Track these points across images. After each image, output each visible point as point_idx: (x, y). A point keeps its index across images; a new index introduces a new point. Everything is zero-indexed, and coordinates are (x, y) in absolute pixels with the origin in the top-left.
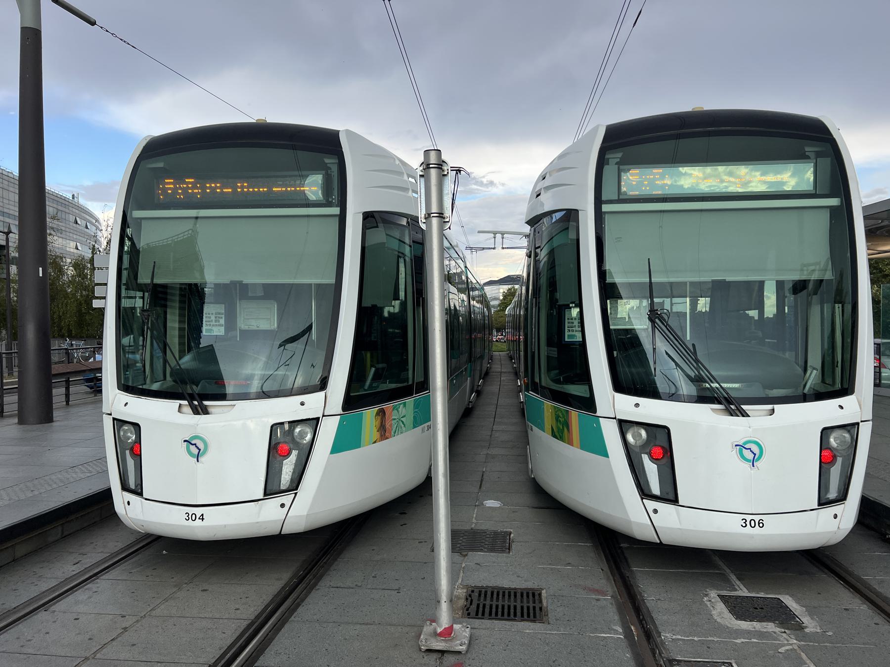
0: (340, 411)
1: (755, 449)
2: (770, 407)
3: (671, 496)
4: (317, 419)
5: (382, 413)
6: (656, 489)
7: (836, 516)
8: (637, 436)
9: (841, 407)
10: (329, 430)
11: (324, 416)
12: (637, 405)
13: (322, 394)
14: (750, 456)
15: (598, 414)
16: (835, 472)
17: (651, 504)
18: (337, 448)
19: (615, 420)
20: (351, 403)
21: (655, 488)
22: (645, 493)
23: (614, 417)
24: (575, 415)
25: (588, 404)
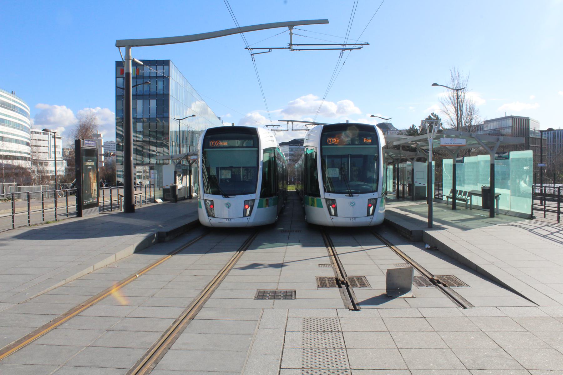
0: (259, 198)
1: (353, 204)
2: (358, 194)
3: (336, 215)
4: (255, 200)
5: (267, 200)
6: (333, 214)
7: (371, 218)
8: (329, 202)
9: (374, 195)
10: (257, 203)
11: (256, 199)
12: (329, 195)
13: (255, 194)
14: (352, 204)
15: (321, 197)
16: (371, 209)
17: (332, 217)
18: (259, 207)
19: (324, 199)
20: (262, 196)
21: (333, 214)
22: (331, 214)
23: (324, 198)
24: (315, 199)
25: (318, 195)
